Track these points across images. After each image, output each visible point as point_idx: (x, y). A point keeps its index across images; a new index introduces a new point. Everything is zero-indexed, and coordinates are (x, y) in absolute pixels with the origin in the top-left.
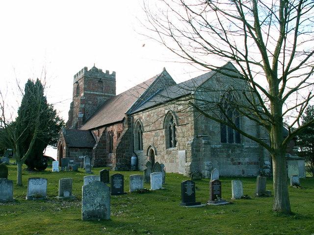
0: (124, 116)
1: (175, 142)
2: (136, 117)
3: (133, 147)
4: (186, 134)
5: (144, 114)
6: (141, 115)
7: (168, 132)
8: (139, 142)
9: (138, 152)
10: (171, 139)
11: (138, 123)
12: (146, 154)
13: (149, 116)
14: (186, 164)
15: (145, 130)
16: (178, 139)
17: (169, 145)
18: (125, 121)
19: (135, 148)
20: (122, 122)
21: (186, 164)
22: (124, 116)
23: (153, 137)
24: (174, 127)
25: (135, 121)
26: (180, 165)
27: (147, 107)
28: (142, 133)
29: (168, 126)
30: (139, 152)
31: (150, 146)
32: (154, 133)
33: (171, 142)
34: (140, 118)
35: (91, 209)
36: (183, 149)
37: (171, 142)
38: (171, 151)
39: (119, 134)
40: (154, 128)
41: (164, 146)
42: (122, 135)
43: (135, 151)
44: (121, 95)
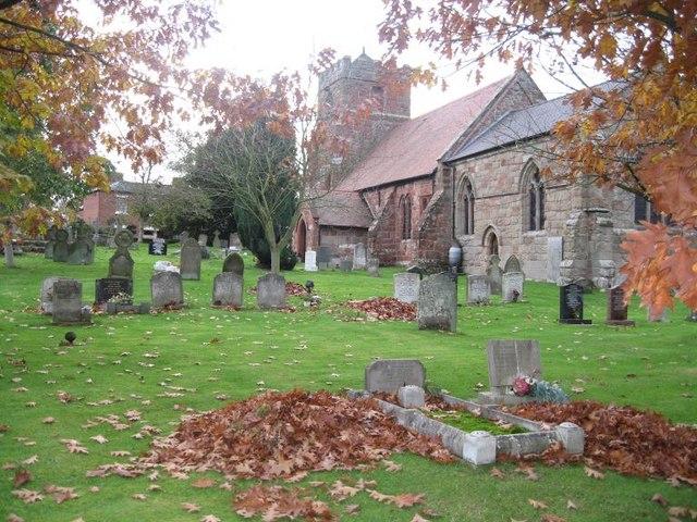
0: (435, 164)
1: (542, 220)
2: (460, 168)
3: (454, 227)
4: (564, 206)
5: (479, 162)
6: (472, 165)
7: (528, 201)
8: (467, 215)
9: (463, 238)
10: (533, 213)
11: (466, 179)
12: (480, 242)
13: (488, 166)
14: (563, 264)
15: (480, 195)
16: (547, 214)
17: (528, 226)
18: (439, 175)
19: (456, 231)
20: (431, 177)
21: (563, 264)
22: (435, 164)
23: (500, 212)
24: (541, 189)
25: (458, 176)
26: (550, 266)
27: (468, 153)
28: (473, 199)
29: (529, 188)
30: (466, 237)
31: (490, 227)
32: (498, 202)
33: (535, 218)
34: (471, 170)
35: (430, 315)
36: (557, 234)
37: (535, 218)
38: (532, 238)
39: (425, 202)
40: (499, 192)
41: (519, 226)
42: (431, 203)
43: (457, 236)
44: (424, 119)
